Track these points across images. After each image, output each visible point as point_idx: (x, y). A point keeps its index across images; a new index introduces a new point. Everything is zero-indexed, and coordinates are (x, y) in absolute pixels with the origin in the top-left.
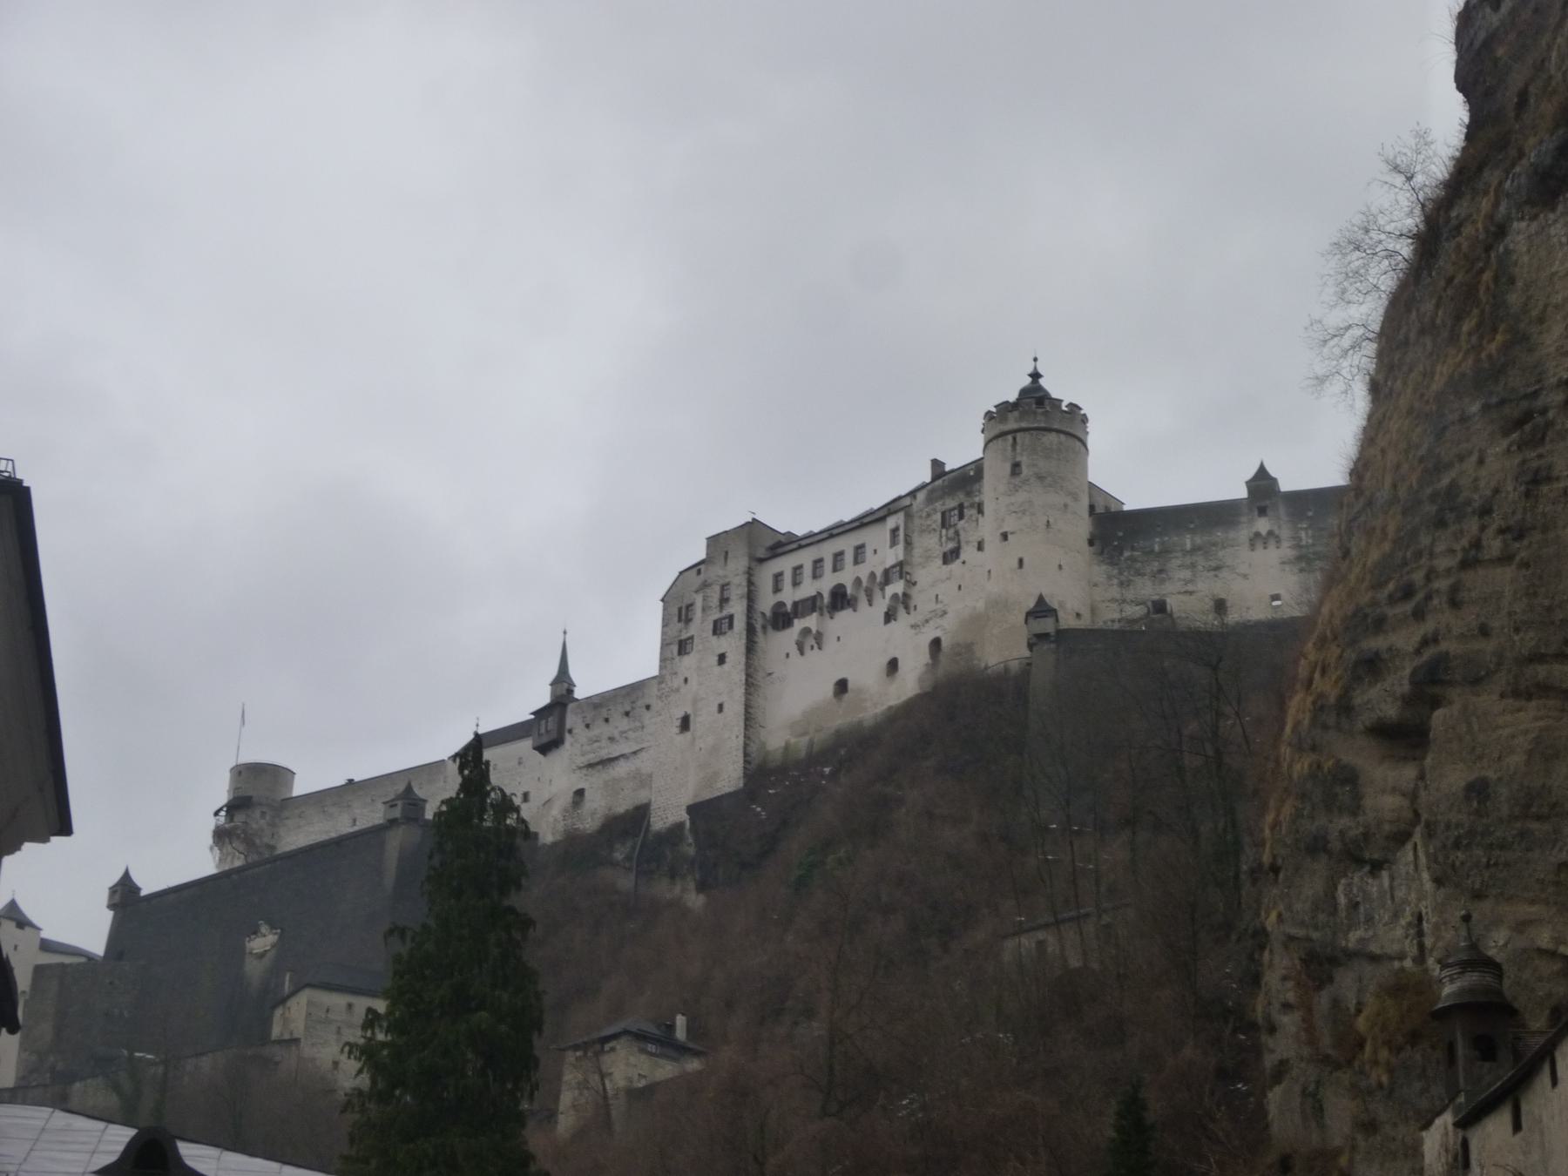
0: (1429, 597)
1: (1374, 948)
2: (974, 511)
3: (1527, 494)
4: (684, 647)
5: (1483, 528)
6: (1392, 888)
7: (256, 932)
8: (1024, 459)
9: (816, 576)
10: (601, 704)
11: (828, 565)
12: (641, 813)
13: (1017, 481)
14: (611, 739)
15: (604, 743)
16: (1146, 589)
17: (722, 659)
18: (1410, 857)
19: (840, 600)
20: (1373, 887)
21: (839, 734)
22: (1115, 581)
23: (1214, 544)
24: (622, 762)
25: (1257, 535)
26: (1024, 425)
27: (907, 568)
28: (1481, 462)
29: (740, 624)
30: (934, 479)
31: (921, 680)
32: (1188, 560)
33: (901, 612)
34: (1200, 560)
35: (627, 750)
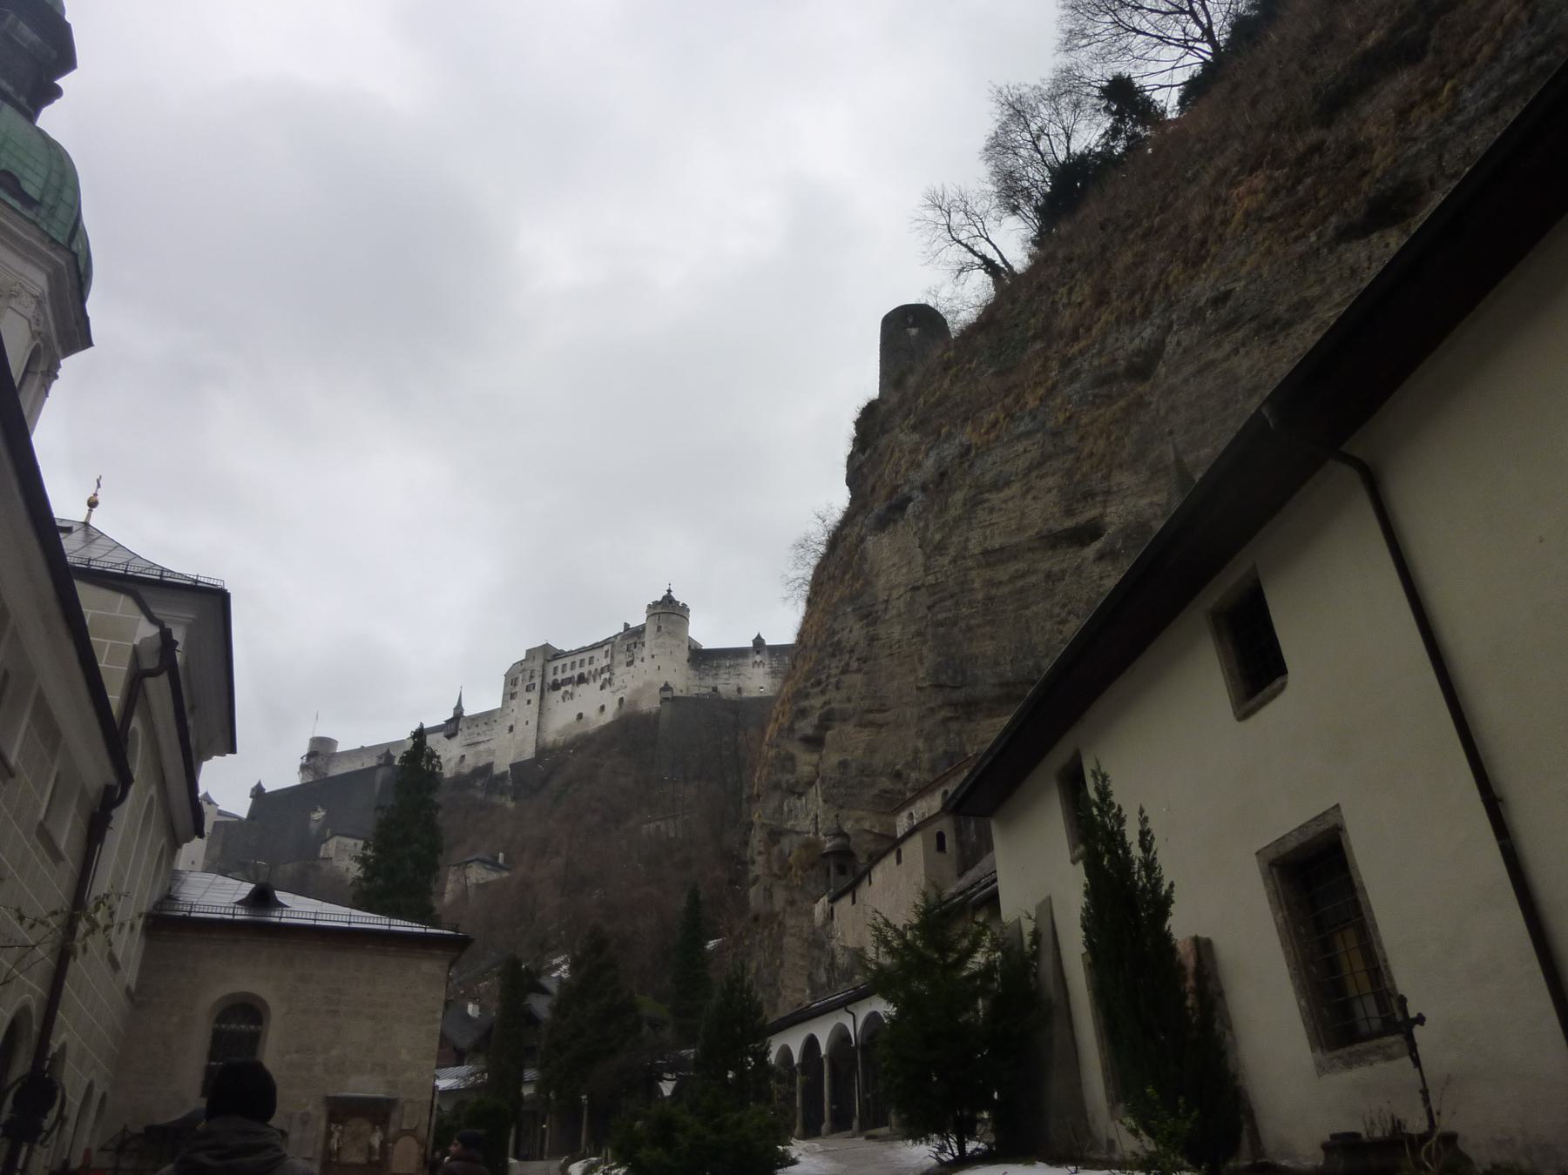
0: (827, 685)
1: (798, 829)
2: (641, 645)
3: (869, 645)
4: (513, 696)
5: (850, 658)
6: (806, 804)
8: (663, 625)
9: (572, 669)
10: (475, 719)
11: (578, 664)
12: (489, 766)
14: (478, 734)
17: (529, 702)
18: (815, 791)
19: (582, 679)
20: (798, 803)
21: (577, 736)
23: (738, 665)
24: (482, 744)
25: (756, 662)
28: (851, 631)
29: (538, 687)
30: (625, 630)
31: (614, 715)
32: (727, 671)
33: (607, 686)
34: (732, 670)
35: (485, 739)
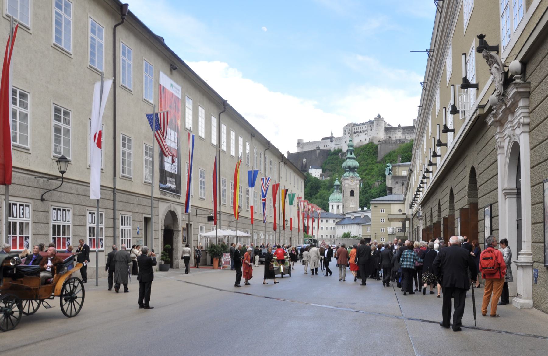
4: (345, 134)
7: (304, 159)
16: (389, 135)
19: (360, 132)
35: (339, 143)
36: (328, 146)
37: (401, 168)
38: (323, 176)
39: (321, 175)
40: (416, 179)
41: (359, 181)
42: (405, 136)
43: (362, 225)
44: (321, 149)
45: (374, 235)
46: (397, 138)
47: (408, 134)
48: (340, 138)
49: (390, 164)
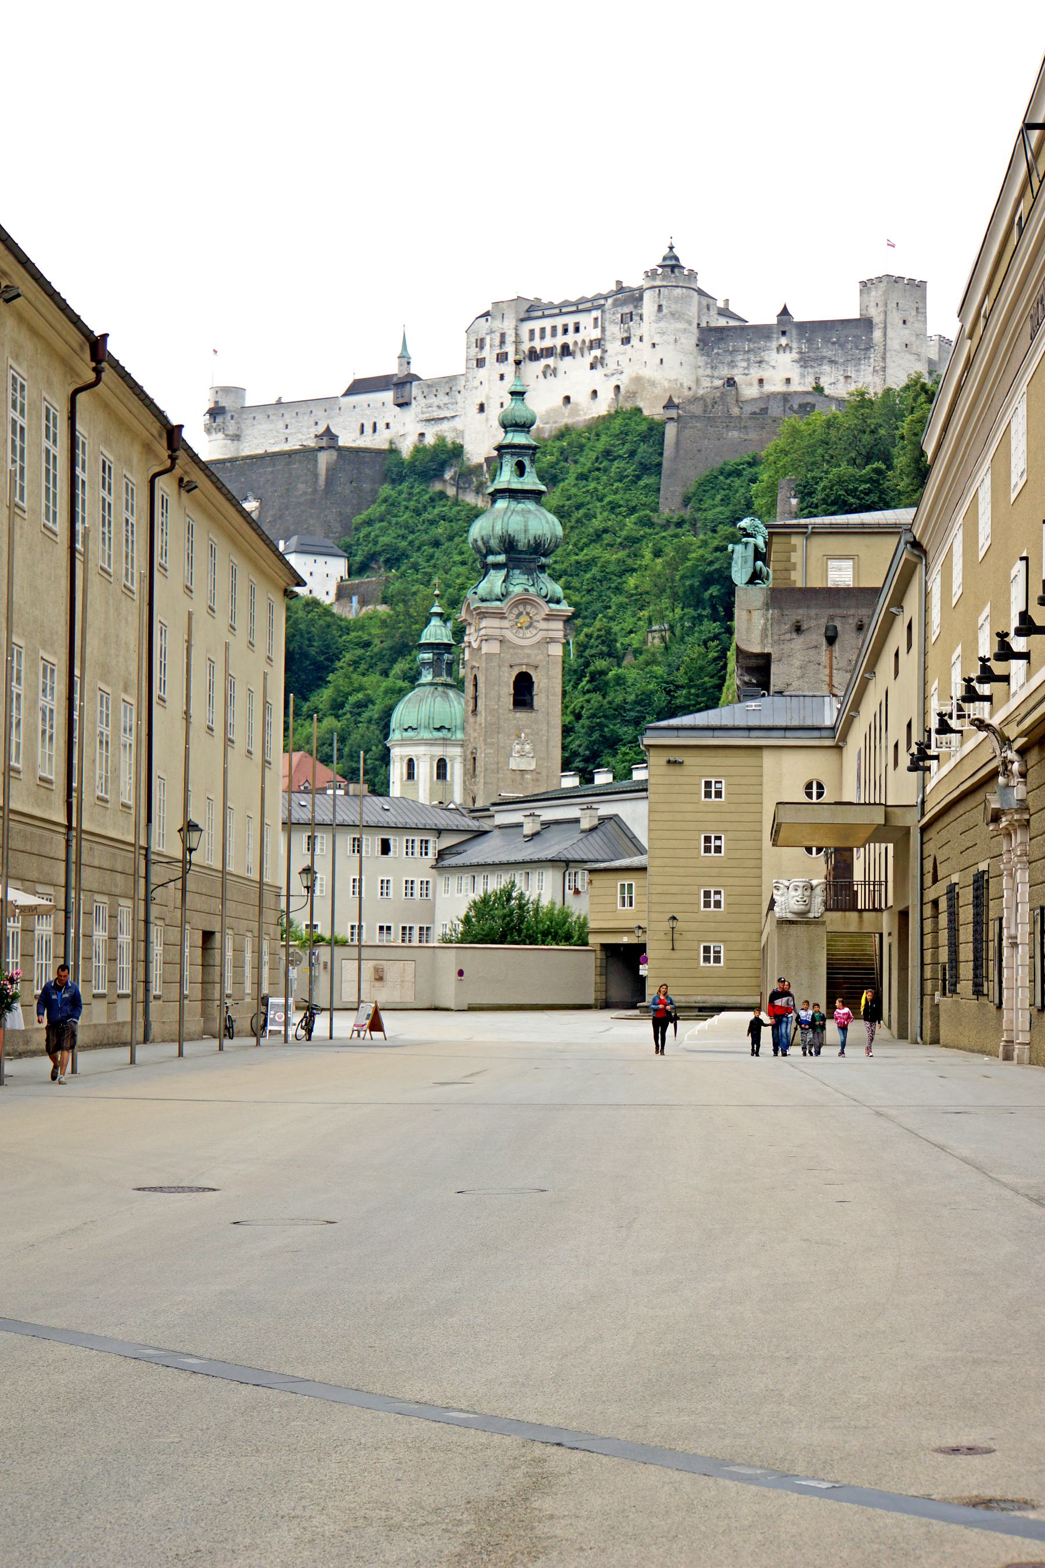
4: (480, 363)
8: (664, 303)
12: (457, 451)
13: (660, 315)
14: (439, 407)
15: (435, 409)
16: (725, 372)
17: (502, 377)
19: (566, 350)
22: (709, 366)
23: (759, 349)
24: (446, 422)
25: (781, 345)
26: (665, 283)
27: (602, 342)
31: (610, 406)
33: (599, 366)
35: (448, 415)
36: (380, 426)
37: (820, 546)
38: (355, 599)
39: (342, 593)
40: (957, 590)
41: (560, 625)
42: (817, 379)
43: (591, 871)
44: (341, 443)
45: (667, 926)
46: (768, 388)
47: (831, 362)
48: (449, 384)
49: (757, 522)
